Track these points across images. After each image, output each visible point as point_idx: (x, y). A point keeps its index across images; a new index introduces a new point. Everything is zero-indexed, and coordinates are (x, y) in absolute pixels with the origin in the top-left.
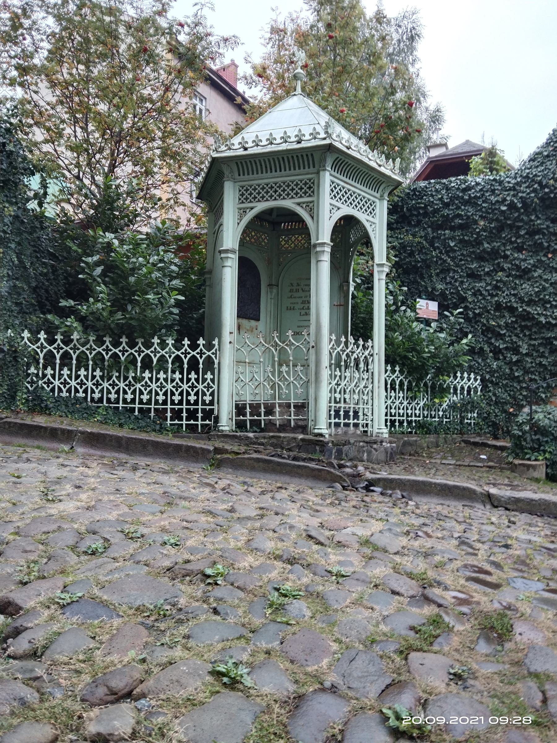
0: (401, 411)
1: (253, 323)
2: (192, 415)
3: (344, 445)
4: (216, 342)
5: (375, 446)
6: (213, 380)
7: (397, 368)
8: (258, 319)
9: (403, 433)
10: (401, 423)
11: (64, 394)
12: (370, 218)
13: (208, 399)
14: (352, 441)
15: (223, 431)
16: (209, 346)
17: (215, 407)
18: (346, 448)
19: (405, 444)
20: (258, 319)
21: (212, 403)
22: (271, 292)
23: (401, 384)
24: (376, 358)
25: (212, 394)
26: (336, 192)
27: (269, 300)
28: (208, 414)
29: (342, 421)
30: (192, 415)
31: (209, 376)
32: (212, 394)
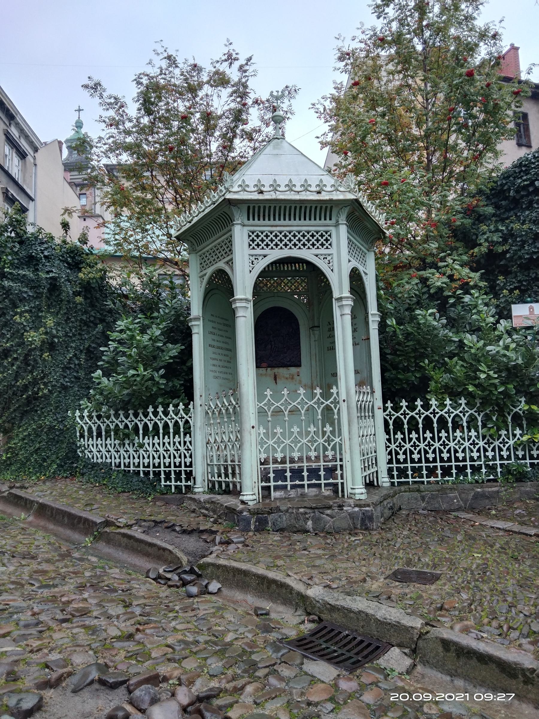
0: (475, 455)
1: (293, 370)
2: (178, 475)
3: (269, 513)
4: (191, 406)
5: (329, 512)
6: (190, 442)
7: (463, 401)
8: (299, 366)
9: (477, 482)
10: (476, 470)
11: (100, 461)
12: (322, 251)
13: (188, 460)
14: (283, 508)
15: (195, 493)
16: (187, 411)
17: (193, 469)
18: (270, 518)
19: (477, 496)
20: (299, 366)
21: (191, 466)
22: (314, 334)
23: (472, 420)
24: (344, 407)
25: (191, 457)
26: (255, 241)
27: (313, 343)
28: (189, 475)
29: (289, 483)
30: (178, 475)
31: (188, 439)
32: (191, 457)
